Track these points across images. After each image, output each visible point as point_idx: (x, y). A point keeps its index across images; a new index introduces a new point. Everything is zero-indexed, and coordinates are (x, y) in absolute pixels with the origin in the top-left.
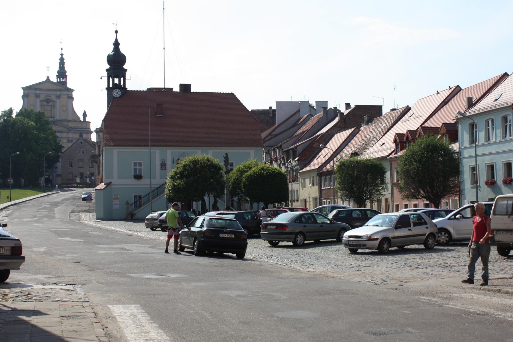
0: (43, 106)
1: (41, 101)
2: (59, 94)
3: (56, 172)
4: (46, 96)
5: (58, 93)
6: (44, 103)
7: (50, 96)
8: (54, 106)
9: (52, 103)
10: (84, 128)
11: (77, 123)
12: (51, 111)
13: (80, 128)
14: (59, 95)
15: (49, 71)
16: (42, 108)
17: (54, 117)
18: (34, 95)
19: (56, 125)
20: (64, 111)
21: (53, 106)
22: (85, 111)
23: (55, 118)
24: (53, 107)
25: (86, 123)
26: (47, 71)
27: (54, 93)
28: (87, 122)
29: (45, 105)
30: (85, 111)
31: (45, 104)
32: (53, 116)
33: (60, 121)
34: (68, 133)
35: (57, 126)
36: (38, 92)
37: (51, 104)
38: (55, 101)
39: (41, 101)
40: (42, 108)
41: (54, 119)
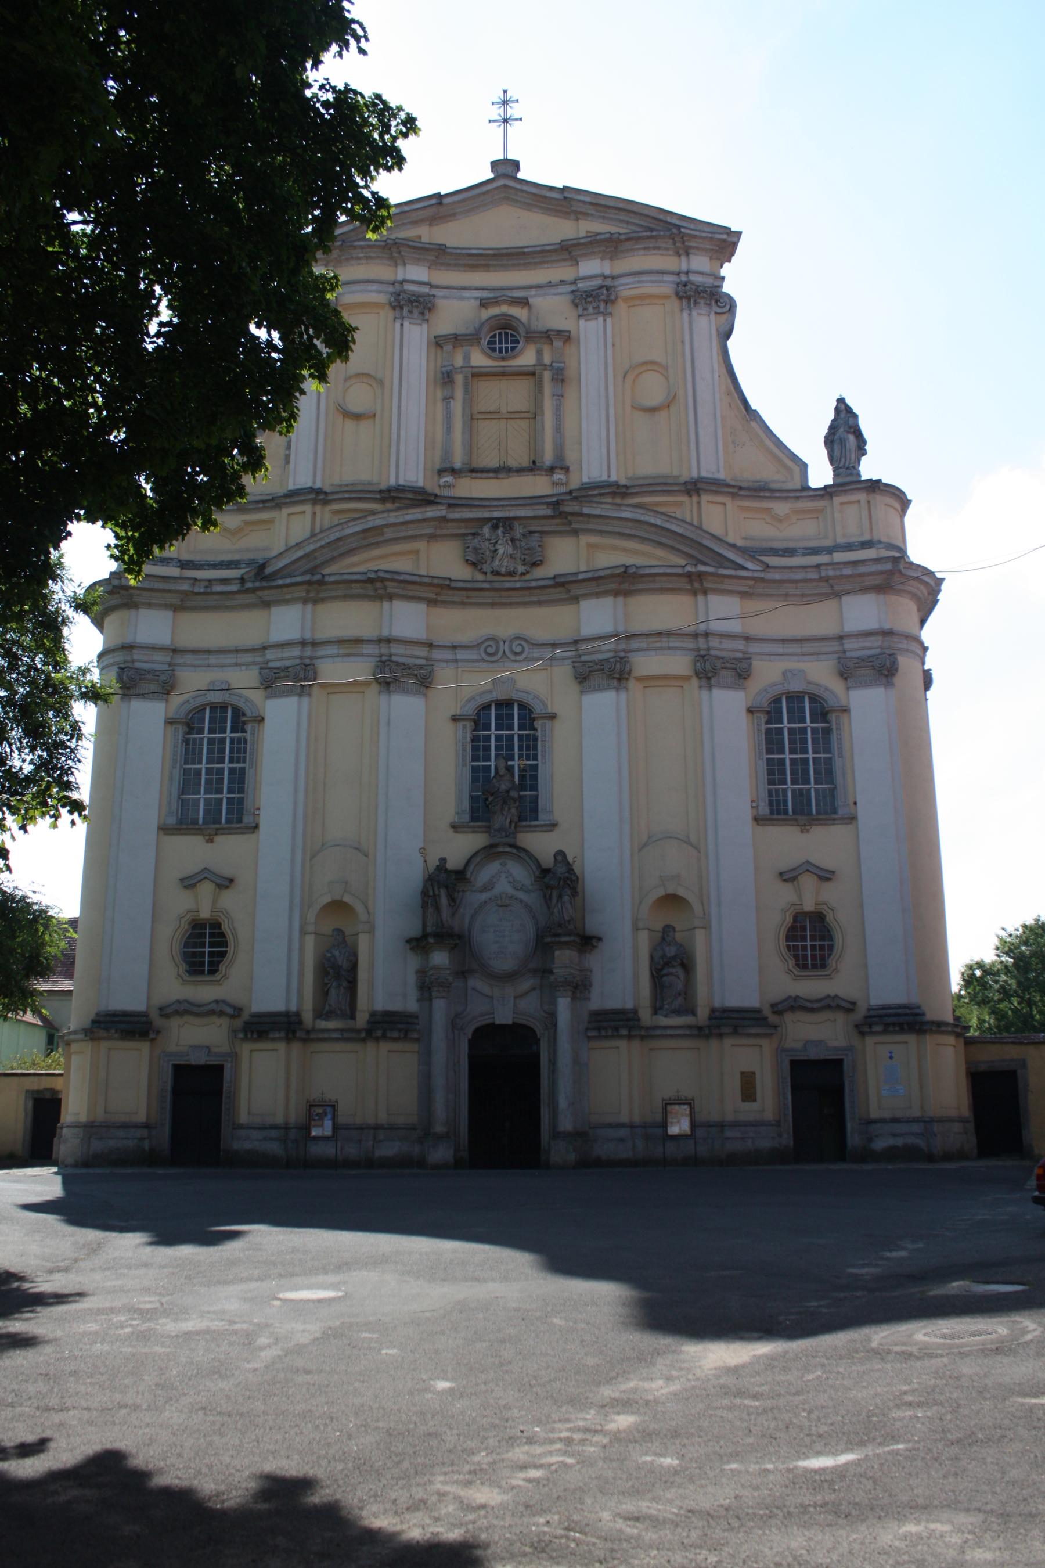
0: (459, 379)
1: (438, 342)
2: (605, 277)
3: (580, 987)
4: (484, 304)
5: (591, 267)
6: (467, 357)
7: (524, 302)
8: (560, 377)
9: (539, 353)
10: (849, 547)
11: (781, 508)
12: (534, 416)
13: (815, 551)
14: (599, 282)
15: (513, 129)
16: (447, 399)
17: (560, 466)
18: (382, 298)
19: (576, 532)
20: (653, 410)
21: (547, 375)
22: (841, 401)
23: (567, 470)
24: (548, 388)
25: (862, 497)
26: (497, 130)
27: (562, 272)
28: (875, 486)
29: (479, 374)
30: (841, 401)
31: (479, 359)
32: (548, 458)
33: (618, 491)
34: (694, 593)
35: (594, 539)
36: (416, 273)
37: (527, 358)
38: (566, 337)
39: (438, 342)
40: (447, 399)
41: (558, 476)
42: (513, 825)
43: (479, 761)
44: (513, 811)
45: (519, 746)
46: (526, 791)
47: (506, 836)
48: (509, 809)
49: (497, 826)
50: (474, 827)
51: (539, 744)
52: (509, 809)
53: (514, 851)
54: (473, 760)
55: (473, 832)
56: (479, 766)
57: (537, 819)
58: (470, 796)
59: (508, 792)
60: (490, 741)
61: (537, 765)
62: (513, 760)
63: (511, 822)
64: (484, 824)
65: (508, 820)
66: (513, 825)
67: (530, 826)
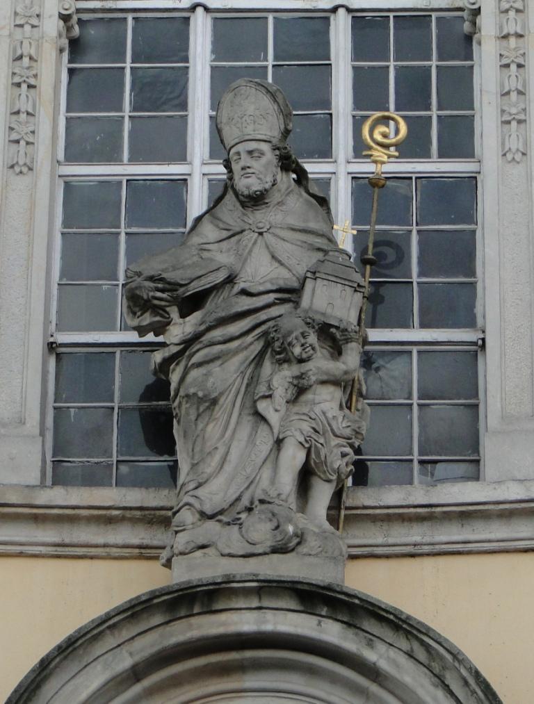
42: (322, 494)
43: (112, 156)
44: (327, 401)
45: (360, 76)
46: (405, 324)
47: (280, 549)
48: (300, 390)
49: (215, 494)
50: (68, 517)
51: (487, 54)
52: (300, 390)
53: (331, 632)
54: (73, 155)
55: (62, 552)
56: (108, 186)
57: (474, 468)
58: (51, 347)
59: (290, 294)
60: (181, 51)
61: (470, 183)
62: (325, 152)
63: (306, 477)
64: (134, 497)
65: (293, 458)
66: (322, 494)
67: (429, 515)
